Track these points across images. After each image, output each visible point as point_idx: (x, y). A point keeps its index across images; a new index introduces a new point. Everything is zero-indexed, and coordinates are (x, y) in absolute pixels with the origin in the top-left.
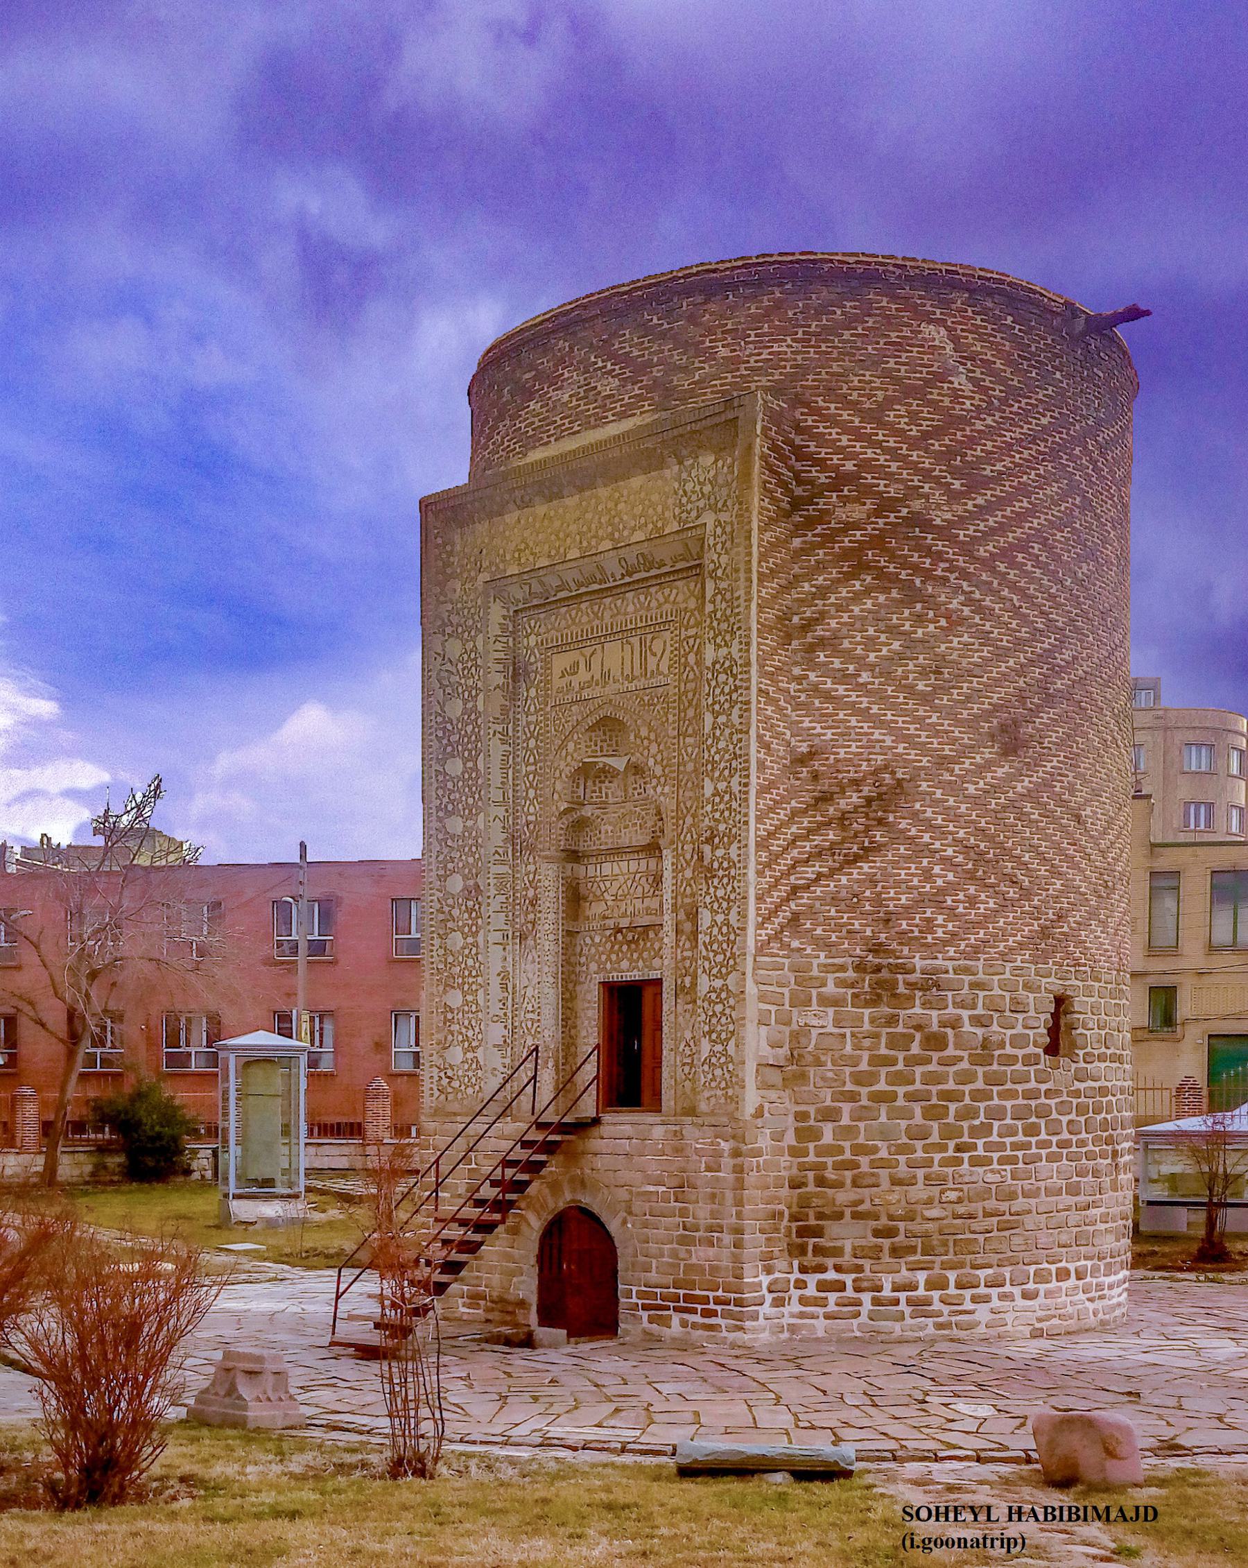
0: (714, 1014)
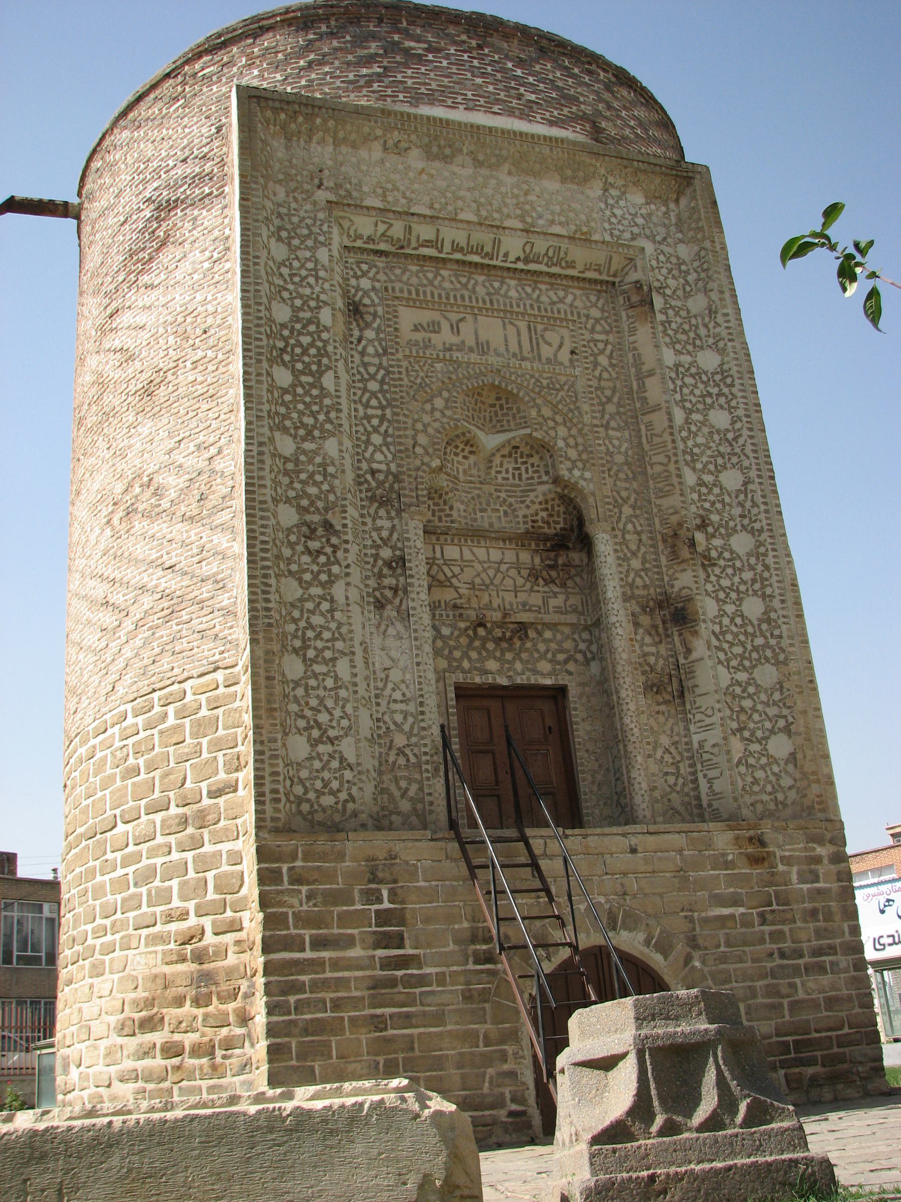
0: (742, 710)
